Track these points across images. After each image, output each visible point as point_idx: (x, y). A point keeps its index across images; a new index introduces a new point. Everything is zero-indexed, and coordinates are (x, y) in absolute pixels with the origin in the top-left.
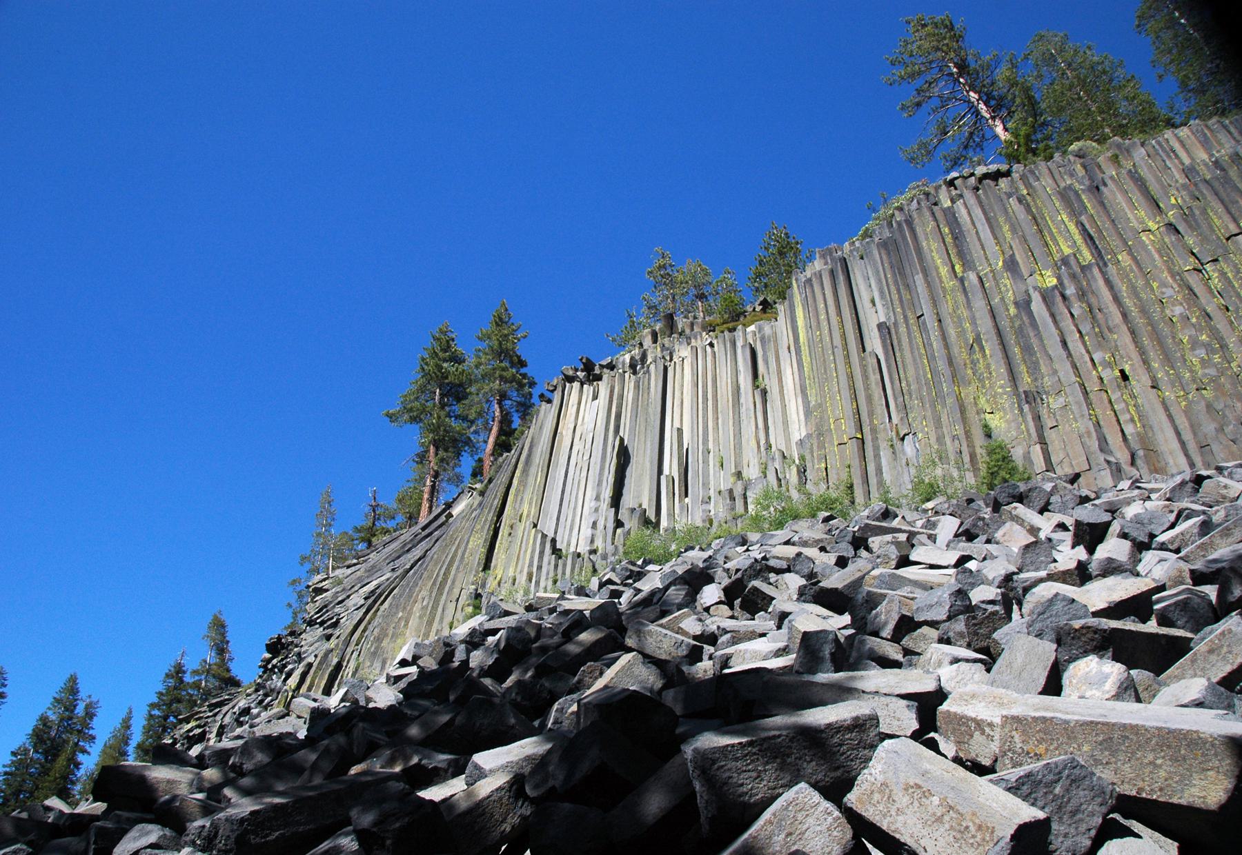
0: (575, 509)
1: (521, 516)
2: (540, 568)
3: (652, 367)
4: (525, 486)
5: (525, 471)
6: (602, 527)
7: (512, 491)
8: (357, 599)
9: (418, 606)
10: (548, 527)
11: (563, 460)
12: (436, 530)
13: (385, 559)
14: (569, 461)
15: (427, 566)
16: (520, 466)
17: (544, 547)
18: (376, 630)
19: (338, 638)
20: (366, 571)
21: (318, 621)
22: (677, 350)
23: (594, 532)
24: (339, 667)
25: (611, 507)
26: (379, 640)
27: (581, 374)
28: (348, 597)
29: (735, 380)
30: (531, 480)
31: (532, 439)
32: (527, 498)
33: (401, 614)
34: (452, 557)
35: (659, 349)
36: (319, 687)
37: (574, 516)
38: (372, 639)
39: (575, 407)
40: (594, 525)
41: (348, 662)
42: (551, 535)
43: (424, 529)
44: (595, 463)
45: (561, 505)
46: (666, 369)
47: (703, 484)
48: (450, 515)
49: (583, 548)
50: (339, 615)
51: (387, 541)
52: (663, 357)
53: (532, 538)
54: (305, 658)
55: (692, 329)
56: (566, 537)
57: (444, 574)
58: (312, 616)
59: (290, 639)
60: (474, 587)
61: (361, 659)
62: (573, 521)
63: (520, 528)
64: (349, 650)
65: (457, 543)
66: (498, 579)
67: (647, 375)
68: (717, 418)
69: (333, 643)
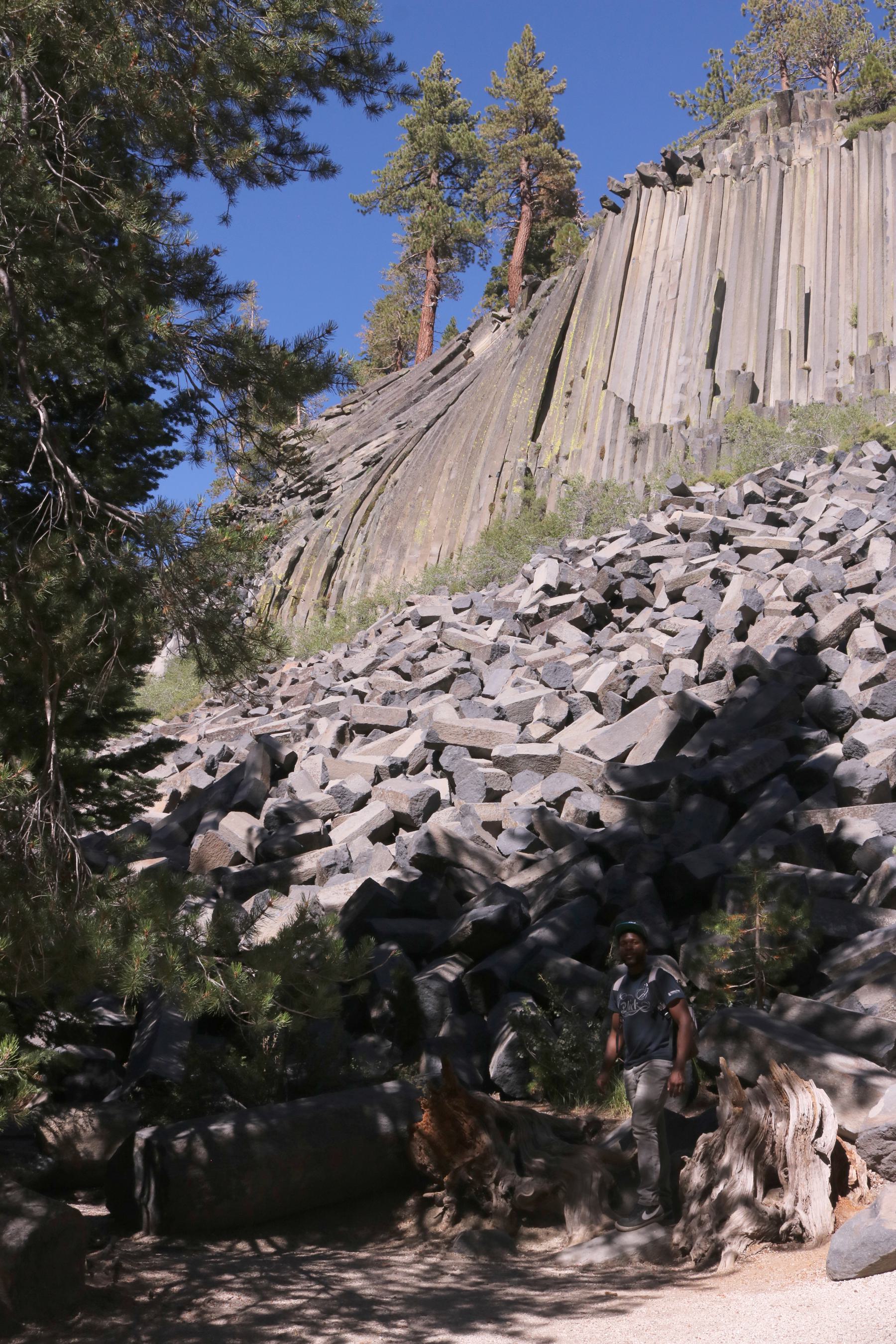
0: (657, 365)
1: (584, 371)
2: (614, 442)
3: (764, 171)
4: (587, 329)
5: (587, 309)
6: (695, 393)
7: (570, 334)
8: (351, 465)
9: (444, 479)
10: (621, 386)
11: (641, 299)
12: (453, 373)
13: (385, 411)
14: (648, 299)
15: (452, 426)
16: (579, 300)
17: (620, 414)
18: (387, 508)
19: (335, 515)
20: (359, 427)
21: (301, 491)
22: (796, 146)
23: (684, 398)
24: (339, 553)
25: (707, 367)
26: (391, 521)
27: (663, 175)
28: (341, 460)
29: (878, 202)
30: (595, 320)
31: (596, 263)
32: (591, 345)
33: (420, 489)
34: (487, 417)
35: (772, 143)
36: (316, 578)
37: (657, 374)
38: (382, 519)
39: (656, 222)
40: (684, 389)
41: (352, 547)
42: (627, 400)
43: (435, 371)
44: (685, 304)
45: (638, 359)
46: (783, 174)
47: (830, 345)
48: (470, 355)
49: (670, 419)
50: (329, 484)
51: (382, 384)
52: (779, 159)
53: (602, 401)
54: (287, 539)
55: (818, 115)
56: (646, 402)
57: (477, 438)
58: (291, 485)
59: (243, 508)
60: (523, 460)
61: (369, 543)
62: (655, 381)
63: (583, 387)
64: (353, 531)
65: (491, 398)
66: (556, 451)
67: (756, 183)
68: (852, 255)
69: (327, 522)
